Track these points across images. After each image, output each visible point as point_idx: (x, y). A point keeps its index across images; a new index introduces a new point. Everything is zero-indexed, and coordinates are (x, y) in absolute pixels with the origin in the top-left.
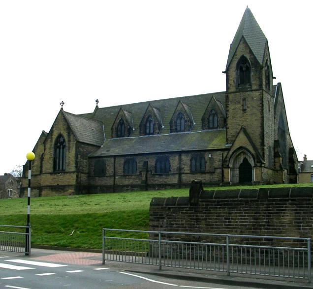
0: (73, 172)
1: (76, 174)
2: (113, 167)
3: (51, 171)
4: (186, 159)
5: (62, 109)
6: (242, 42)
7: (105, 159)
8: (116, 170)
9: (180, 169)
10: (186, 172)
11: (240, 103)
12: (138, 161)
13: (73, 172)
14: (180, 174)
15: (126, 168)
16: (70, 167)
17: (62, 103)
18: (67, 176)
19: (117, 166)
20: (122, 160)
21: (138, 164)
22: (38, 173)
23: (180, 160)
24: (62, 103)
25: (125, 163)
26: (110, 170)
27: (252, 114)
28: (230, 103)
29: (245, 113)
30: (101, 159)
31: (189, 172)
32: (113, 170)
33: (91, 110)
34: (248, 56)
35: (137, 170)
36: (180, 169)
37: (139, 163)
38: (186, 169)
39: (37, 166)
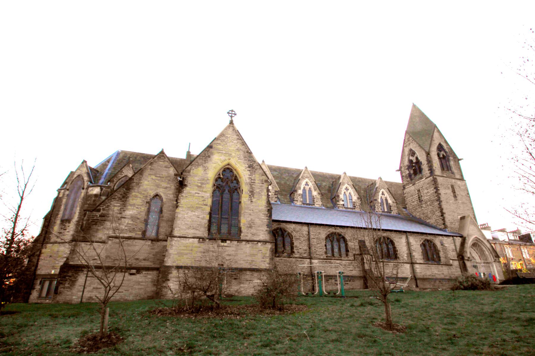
0: (265, 242)
1: (269, 246)
2: (307, 243)
3: (203, 232)
4: (416, 243)
5: (231, 122)
6: (436, 131)
7: (293, 226)
8: (313, 249)
9: (410, 254)
10: (418, 262)
11: (449, 188)
12: (347, 237)
13: (265, 242)
14: (412, 264)
15: (329, 247)
16: (253, 231)
17: (232, 113)
18: (246, 248)
19: (314, 242)
20: (323, 233)
21: (350, 244)
22: (139, 234)
23: (408, 243)
24: (232, 113)
25: (328, 237)
26: (300, 246)
27: (463, 203)
28: (439, 186)
29: (457, 200)
30: (283, 225)
31: (422, 262)
32: (306, 248)
33: (191, 153)
34: (445, 147)
35: (347, 251)
36: (410, 254)
37: (350, 240)
38: (418, 255)
39: (133, 218)
